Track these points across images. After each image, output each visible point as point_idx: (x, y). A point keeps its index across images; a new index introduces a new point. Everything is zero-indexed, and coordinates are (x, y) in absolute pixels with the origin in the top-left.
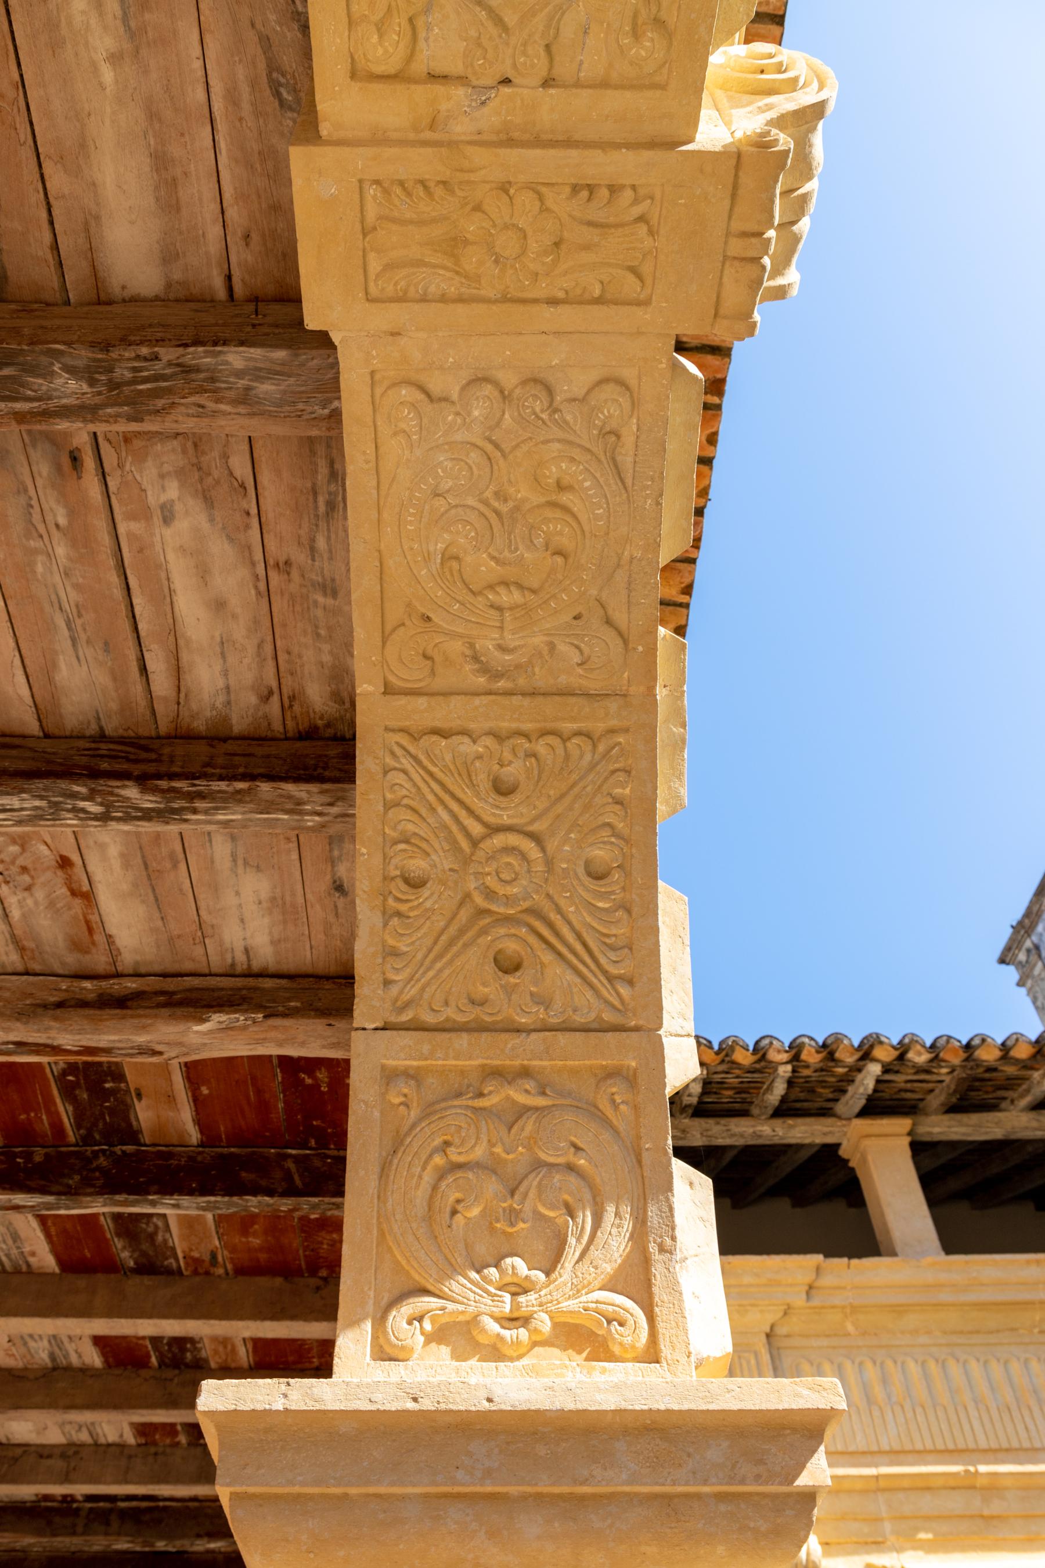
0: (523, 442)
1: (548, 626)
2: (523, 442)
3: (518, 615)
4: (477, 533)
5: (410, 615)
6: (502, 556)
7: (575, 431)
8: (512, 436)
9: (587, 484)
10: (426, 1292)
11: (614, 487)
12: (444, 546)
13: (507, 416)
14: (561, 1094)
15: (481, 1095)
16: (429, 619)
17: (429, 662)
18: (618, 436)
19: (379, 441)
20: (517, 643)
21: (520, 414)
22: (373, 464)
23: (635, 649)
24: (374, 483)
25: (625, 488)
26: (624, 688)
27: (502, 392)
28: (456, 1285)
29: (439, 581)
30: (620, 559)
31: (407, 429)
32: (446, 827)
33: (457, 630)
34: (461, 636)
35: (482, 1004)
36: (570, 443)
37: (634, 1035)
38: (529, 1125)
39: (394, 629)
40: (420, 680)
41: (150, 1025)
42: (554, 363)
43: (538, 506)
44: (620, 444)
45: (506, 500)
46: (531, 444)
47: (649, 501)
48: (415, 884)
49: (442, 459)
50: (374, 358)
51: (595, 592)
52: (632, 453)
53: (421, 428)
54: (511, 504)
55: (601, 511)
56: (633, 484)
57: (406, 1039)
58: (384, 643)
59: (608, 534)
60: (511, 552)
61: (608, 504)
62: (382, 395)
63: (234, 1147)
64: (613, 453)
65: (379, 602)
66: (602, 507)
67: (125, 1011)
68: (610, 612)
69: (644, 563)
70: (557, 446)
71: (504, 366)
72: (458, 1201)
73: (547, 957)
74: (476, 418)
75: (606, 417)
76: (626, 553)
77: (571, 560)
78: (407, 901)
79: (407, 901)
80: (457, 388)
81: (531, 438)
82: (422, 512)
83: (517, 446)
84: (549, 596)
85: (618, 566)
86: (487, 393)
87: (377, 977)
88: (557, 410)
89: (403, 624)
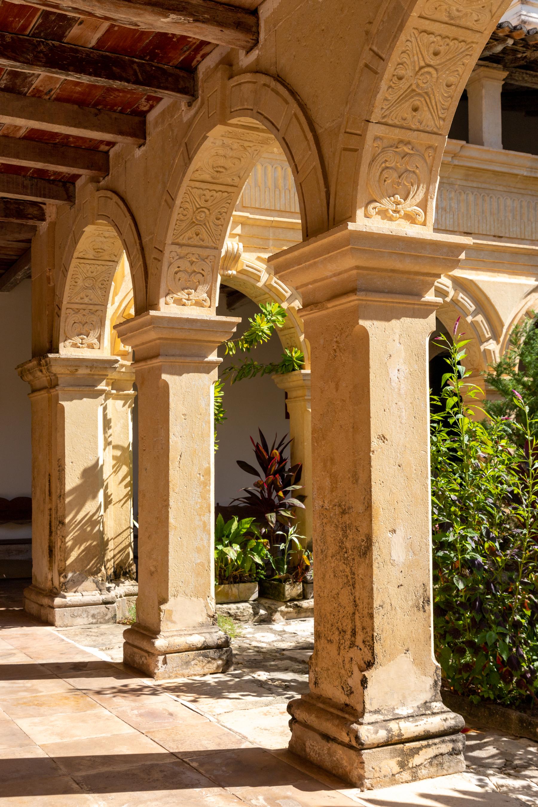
10: (376, 201)
14: (417, 151)
15: (397, 147)
28: (384, 201)
32: (414, 62)
35: (405, 120)
37: (440, 137)
38: (407, 158)
41: (142, 14)
48: (400, 78)
57: (383, 127)
63: (108, 52)
67: (130, 4)
72: (386, 178)
73: (426, 109)
78: (395, 84)
79: (395, 84)
87: (380, 107)
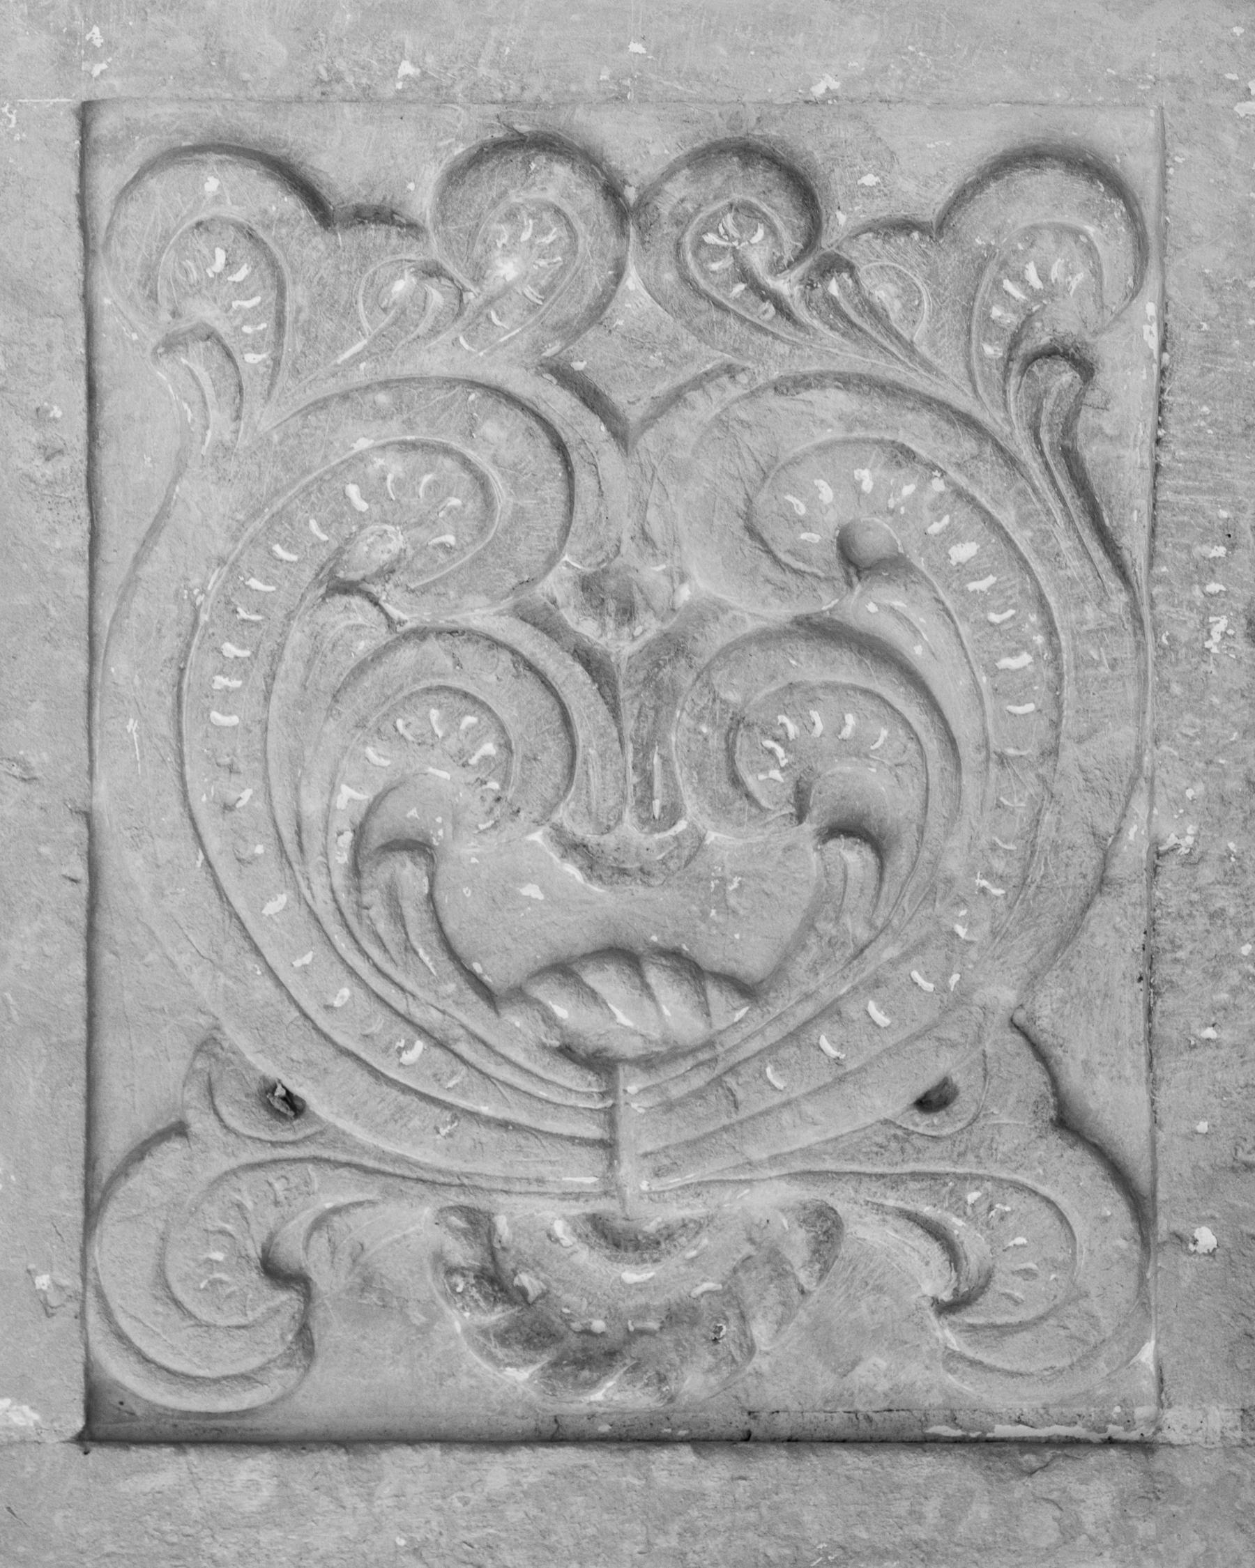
0: (698, 383)
1: (809, 1137)
2: (698, 383)
3: (676, 1092)
4: (507, 746)
5: (210, 1090)
6: (610, 841)
7: (910, 348)
8: (655, 360)
9: (963, 552)
11: (1075, 567)
12: (365, 797)
13: (632, 281)
16: (293, 1106)
17: (287, 1299)
18: (1086, 369)
19: (103, 368)
20: (675, 1212)
21: (686, 280)
22: (75, 460)
23: (1180, 1239)
24: (78, 537)
25: (1121, 570)
26: (1142, 1412)
27: (612, 191)
29: (342, 943)
30: (1105, 863)
31: (223, 328)
33: (416, 1155)
34: (431, 1182)
36: (891, 391)
39: (141, 1152)
40: (246, 1378)
42: (819, 90)
43: (766, 638)
44: (1094, 397)
45: (627, 613)
46: (734, 391)
47: (1220, 625)
49: (363, 444)
50: (93, 53)
51: (1007, 996)
52: (1143, 431)
53: (280, 324)
54: (649, 627)
55: (1025, 659)
56: (1152, 556)
58: (92, 1212)
59: (1052, 752)
60: (648, 822)
61: (1051, 631)
62: (124, 193)
64: (1068, 429)
65: (79, 1033)
66: (1025, 645)
68: (1073, 1078)
69: (1207, 874)
70: (836, 400)
71: (620, 98)
74: (507, 289)
75: (1035, 296)
76: (1132, 832)
77: (901, 860)
80: (432, 174)
81: (730, 371)
82: (276, 657)
83: (677, 397)
84: (808, 1009)
85: (1103, 882)
86: (551, 195)
88: (833, 265)
89: (180, 1130)
